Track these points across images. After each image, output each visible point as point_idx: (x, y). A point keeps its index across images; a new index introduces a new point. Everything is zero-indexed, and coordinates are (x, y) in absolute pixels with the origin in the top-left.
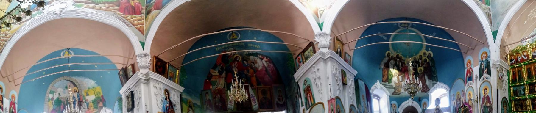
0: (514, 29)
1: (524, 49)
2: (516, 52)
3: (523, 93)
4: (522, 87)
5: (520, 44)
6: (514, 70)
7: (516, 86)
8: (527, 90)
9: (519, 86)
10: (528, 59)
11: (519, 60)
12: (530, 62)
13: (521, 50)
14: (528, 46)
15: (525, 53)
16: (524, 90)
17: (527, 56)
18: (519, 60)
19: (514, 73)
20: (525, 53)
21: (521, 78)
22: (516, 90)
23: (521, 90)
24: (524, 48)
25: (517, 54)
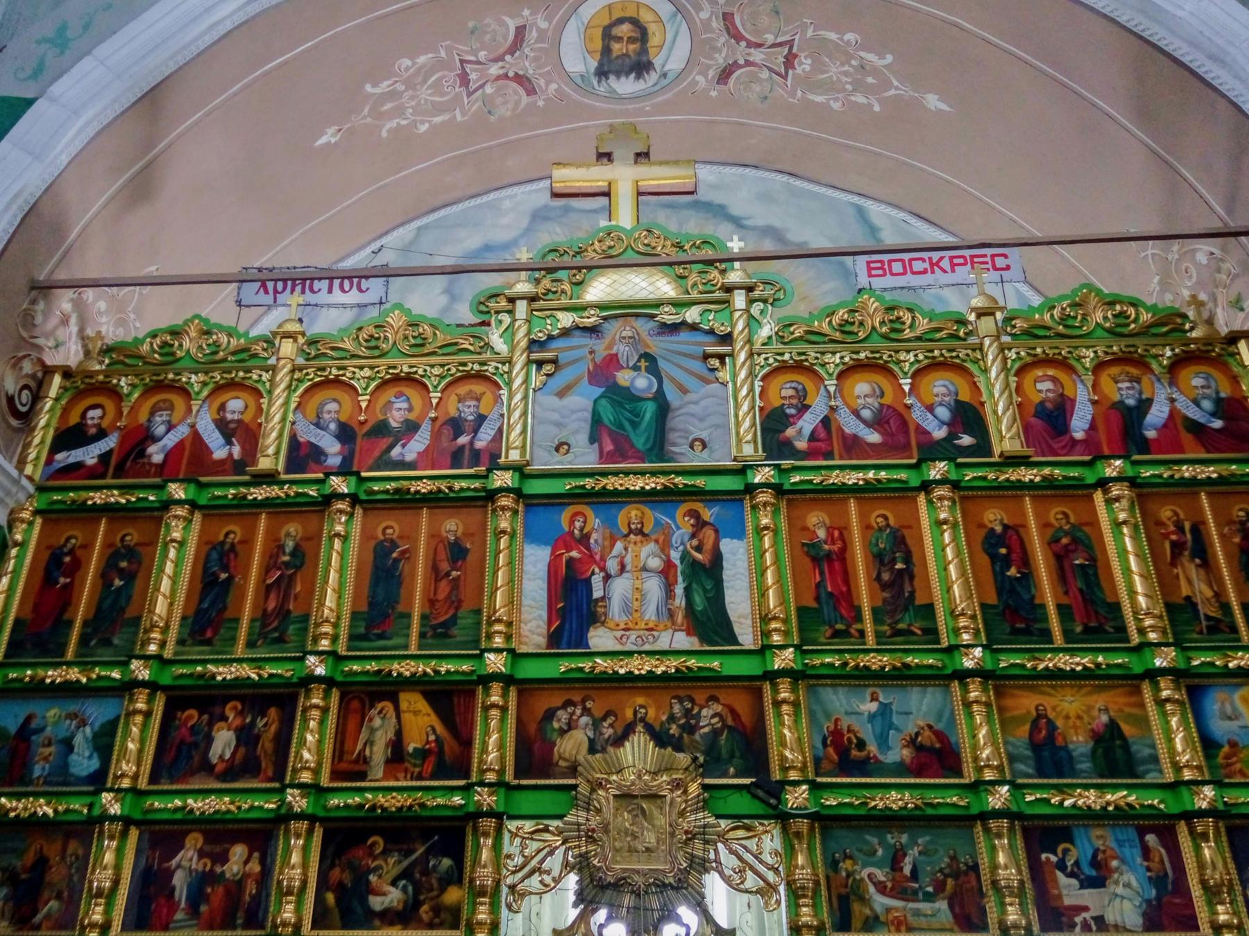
0: (198, 153)
1: (236, 369)
2: (156, 370)
3: (83, 762)
4: (98, 712)
5: (217, 306)
6: (75, 535)
7: (39, 690)
8: (135, 750)
9: (69, 690)
10: (238, 466)
11: (156, 454)
12: (259, 493)
13: (207, 366)
14: (287, 348)
15: (235, 405)
16: (105, 743)
17: (245, 433)
18: (156, 454)
19: (56, 569)
20: (235, 405)
21: (116, 620)
22: (26, 731)
23: (81, 741)
24: (245, 354)
25: (160, 386)
